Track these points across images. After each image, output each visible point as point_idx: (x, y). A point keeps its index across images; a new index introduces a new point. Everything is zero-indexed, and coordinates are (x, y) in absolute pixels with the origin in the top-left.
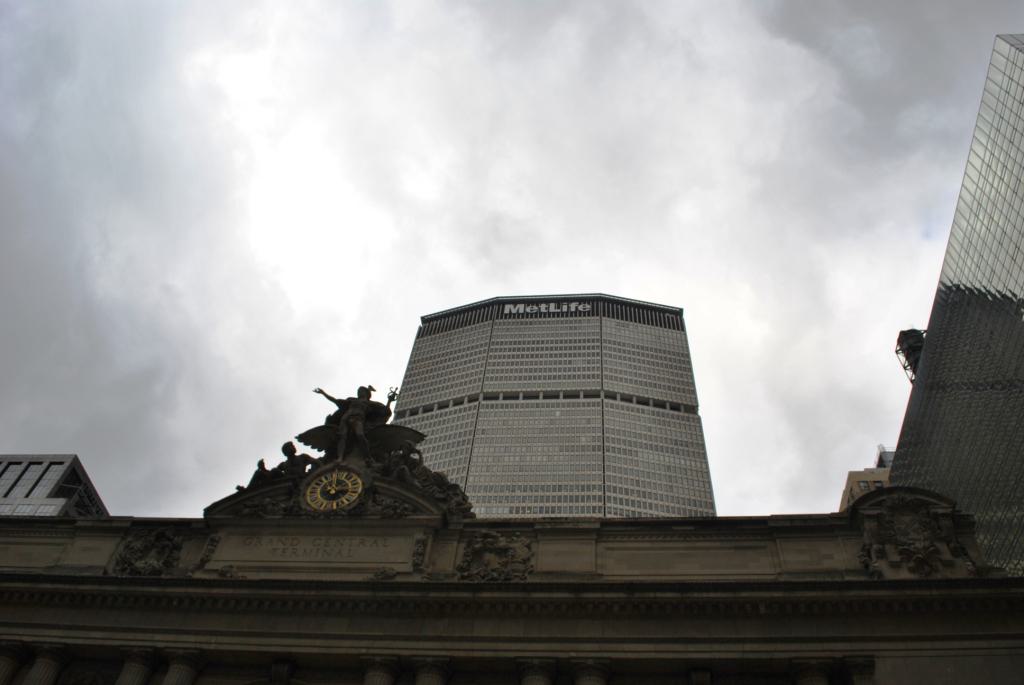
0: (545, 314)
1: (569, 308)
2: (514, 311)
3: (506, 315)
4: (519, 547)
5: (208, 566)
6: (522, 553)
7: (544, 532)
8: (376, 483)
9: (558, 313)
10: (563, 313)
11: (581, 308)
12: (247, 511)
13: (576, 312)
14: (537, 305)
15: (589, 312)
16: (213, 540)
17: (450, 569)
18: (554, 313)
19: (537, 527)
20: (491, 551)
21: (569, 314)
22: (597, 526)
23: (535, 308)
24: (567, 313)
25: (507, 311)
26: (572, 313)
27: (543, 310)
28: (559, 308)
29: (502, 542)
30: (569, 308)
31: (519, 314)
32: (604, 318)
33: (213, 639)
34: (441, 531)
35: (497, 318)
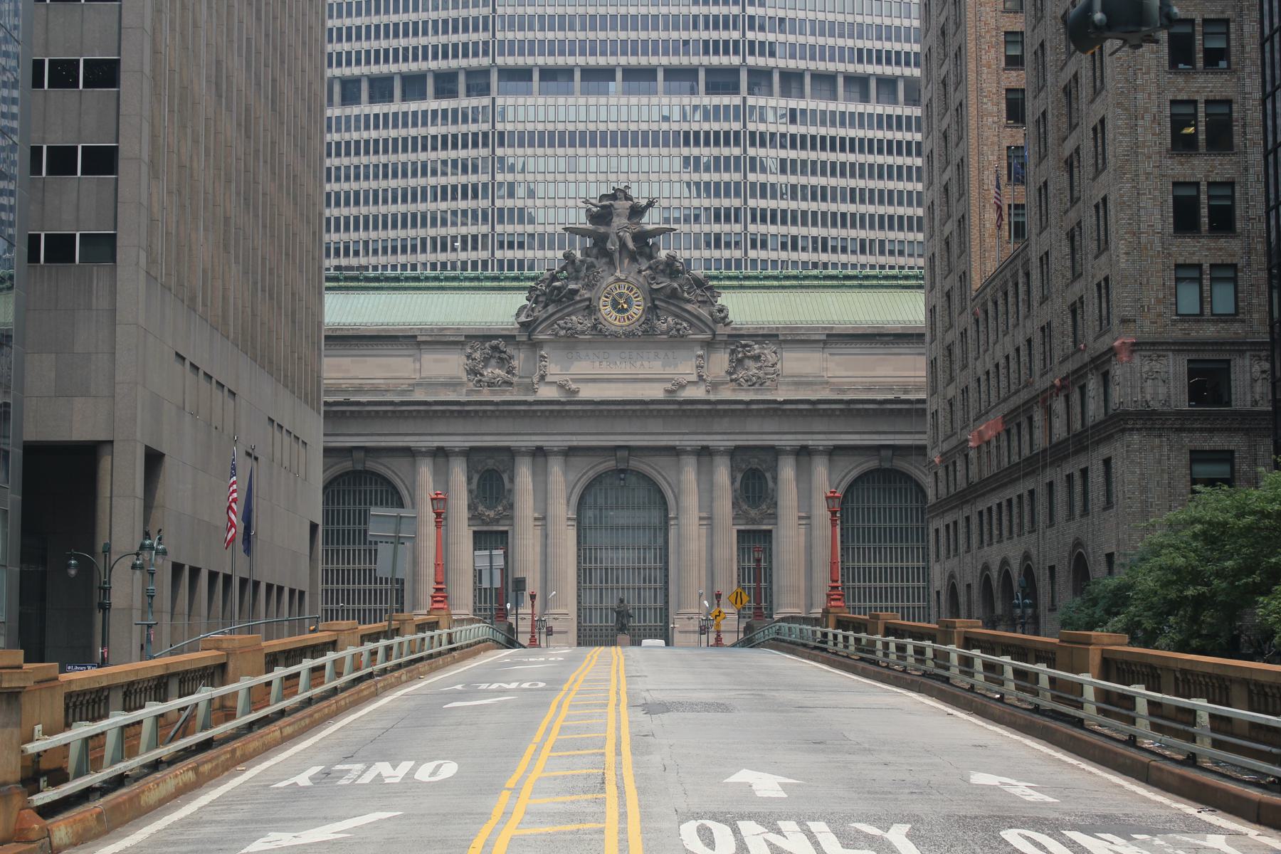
4: (768, 352)
5: (548, 379)
6: (772, 358)
7: (786, 341)
8: (657, 302)
12: (562, 333)
16: (542, 356)
17: (723, 374)
19: (781, 338)
20: (749, 358)
22: (824, 337)
29: (757, 349)
33: (574, 438)
34: (710, 345)
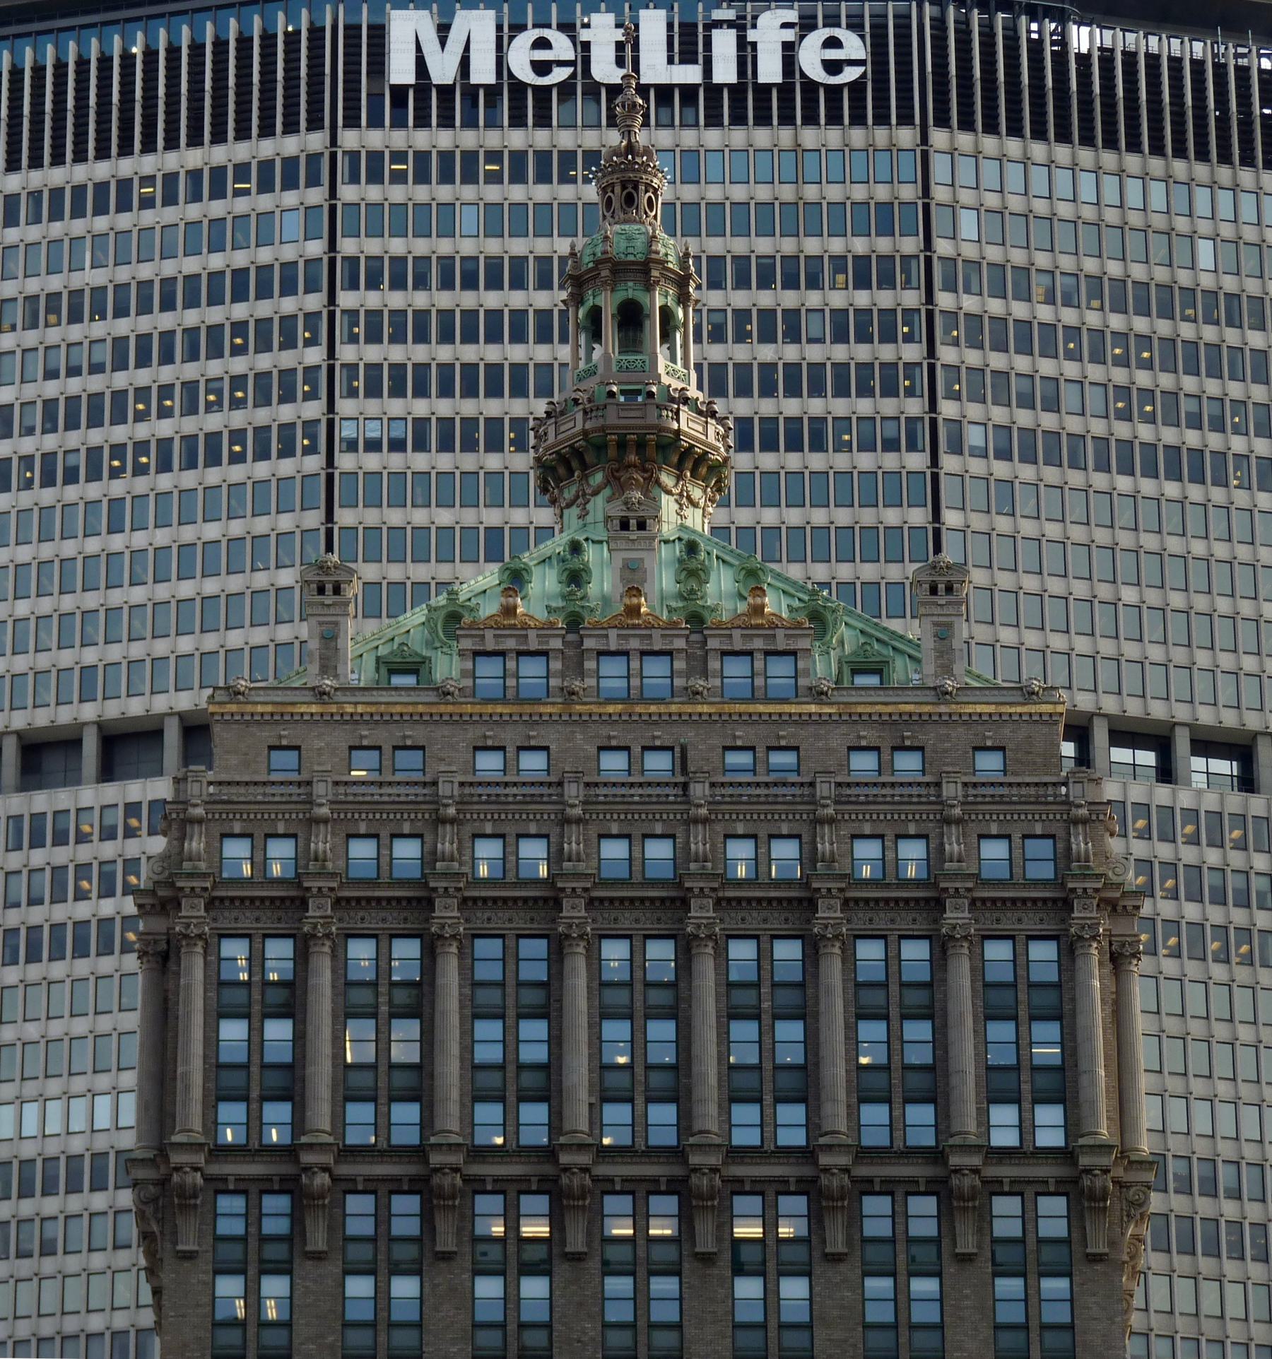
0: (614, 90)
1: (746, 53)
2: (443, 70)
3: (399, 92)
9: (689, 92)
10: (714, 91)
11: (811, 59)
13: (785, 90)
14: (567, 28)
15: (857, 87)
18: (664, 93)
21: (746, 101)
23: (562, 48)
24: (737, 91)
25: (401, 71)
26: (763, 91)
27: (605, 70)
28: (688, 57)
30: (746, 53)
31: (471, 93)
32: (939, 137)
35: (352, 121)
